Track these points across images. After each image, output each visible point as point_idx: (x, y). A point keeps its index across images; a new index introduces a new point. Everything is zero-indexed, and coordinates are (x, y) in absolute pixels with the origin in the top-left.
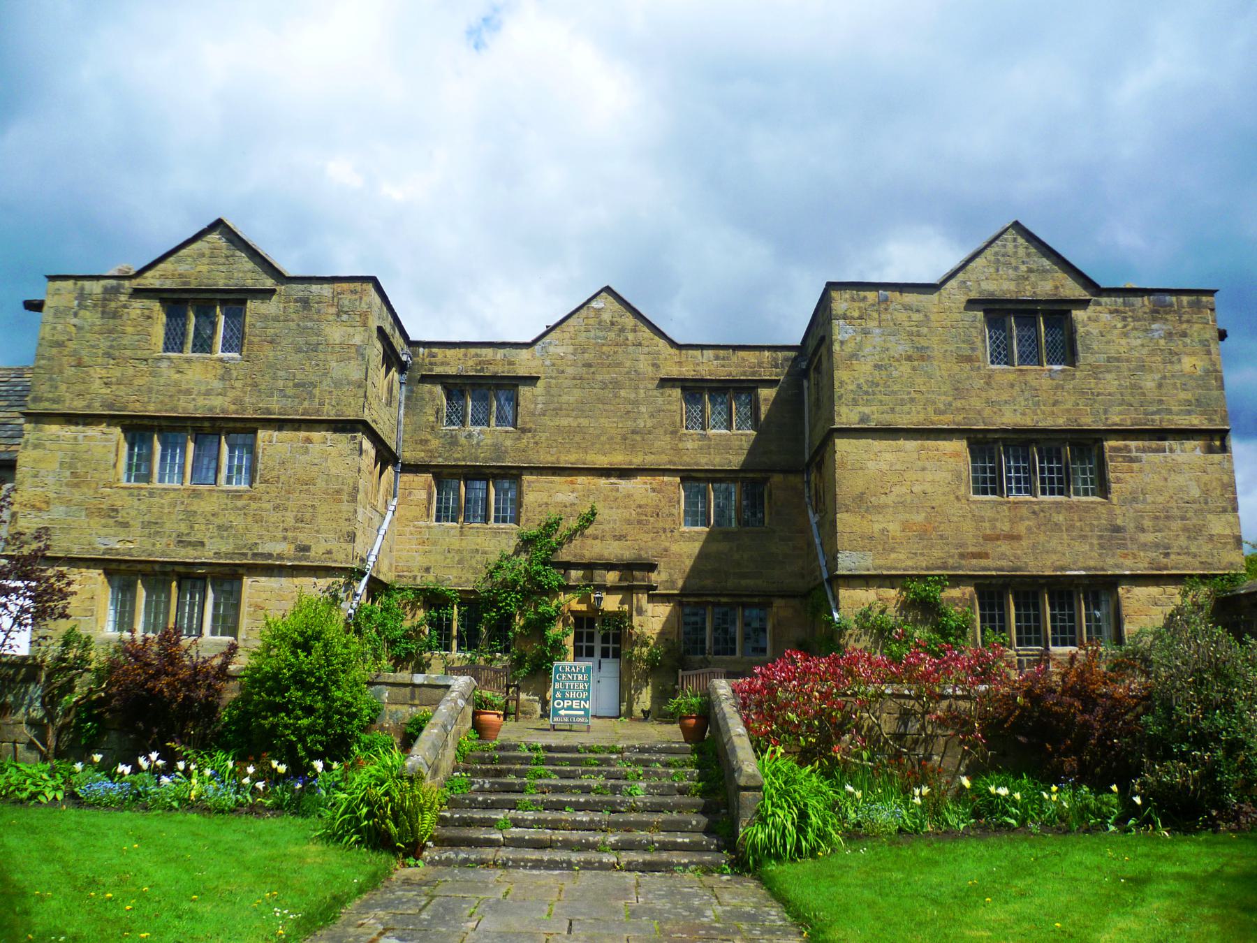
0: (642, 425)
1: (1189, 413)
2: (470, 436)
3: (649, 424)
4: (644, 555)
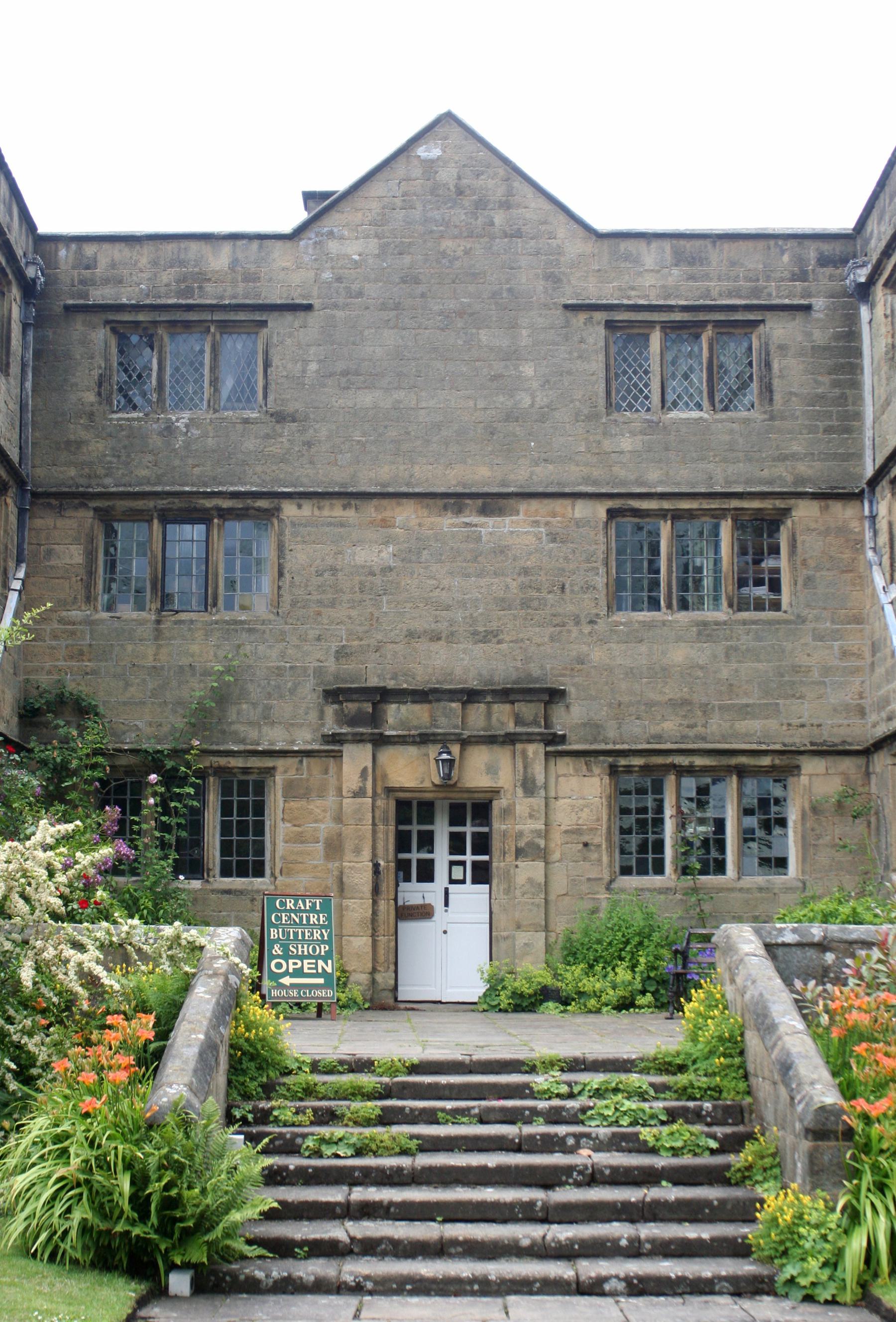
0: (527, 401)
2: (169, 430)
3: (542, 399)
4: (536, 672)
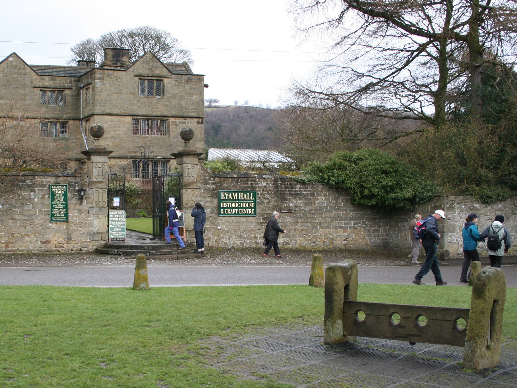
1: (193, 112)
3: (29, 102)
